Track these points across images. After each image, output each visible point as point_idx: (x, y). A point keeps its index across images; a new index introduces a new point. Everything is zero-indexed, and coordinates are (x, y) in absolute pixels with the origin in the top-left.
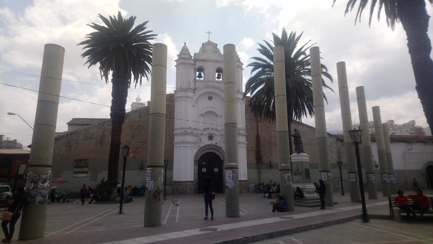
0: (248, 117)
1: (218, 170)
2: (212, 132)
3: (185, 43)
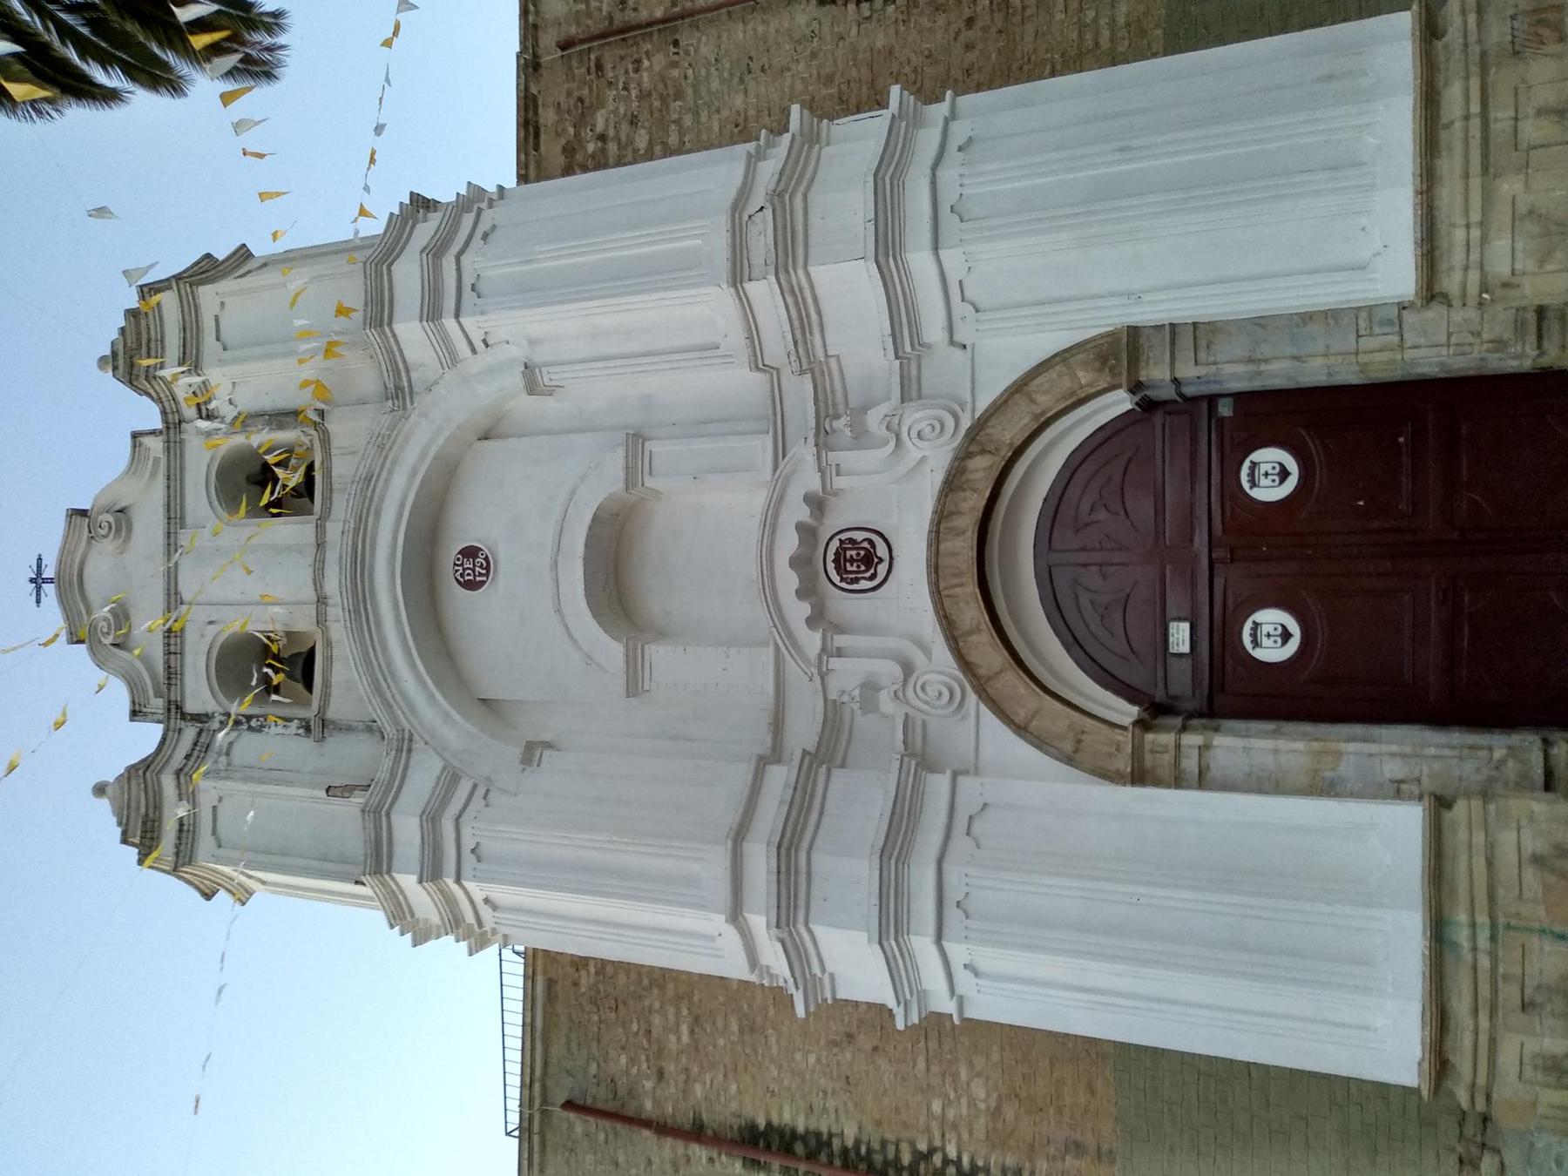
0: (641, 140)
1: (1269, 457)
2: (789, 542)
3: (100, 790)
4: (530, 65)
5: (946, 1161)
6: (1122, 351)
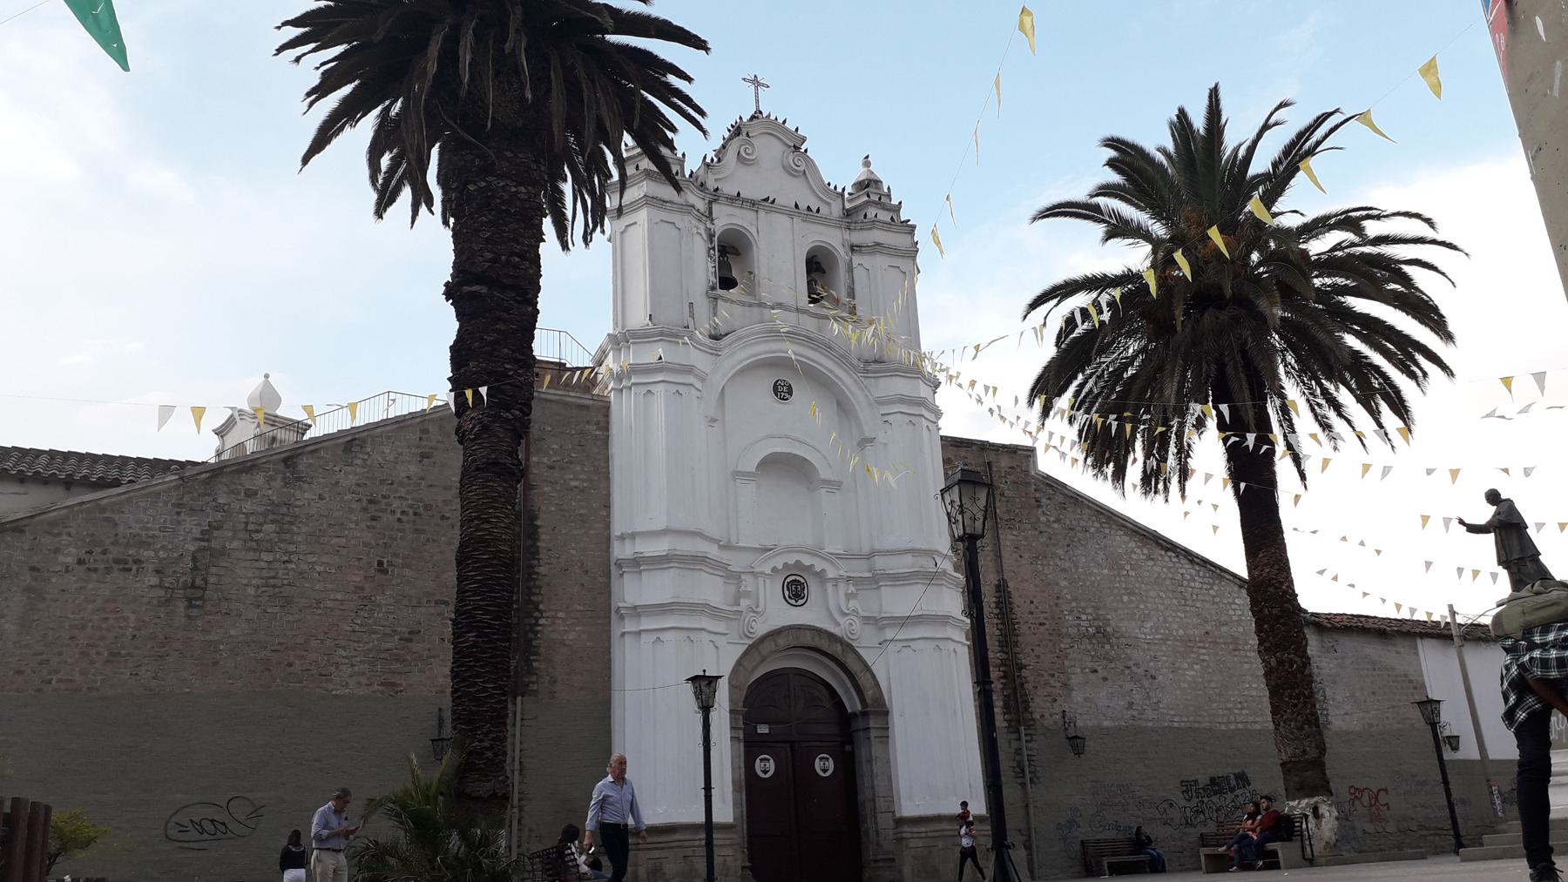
1: (831, 764)
4: (984, 446)
5: (537, 619)
6: (877, 710)
